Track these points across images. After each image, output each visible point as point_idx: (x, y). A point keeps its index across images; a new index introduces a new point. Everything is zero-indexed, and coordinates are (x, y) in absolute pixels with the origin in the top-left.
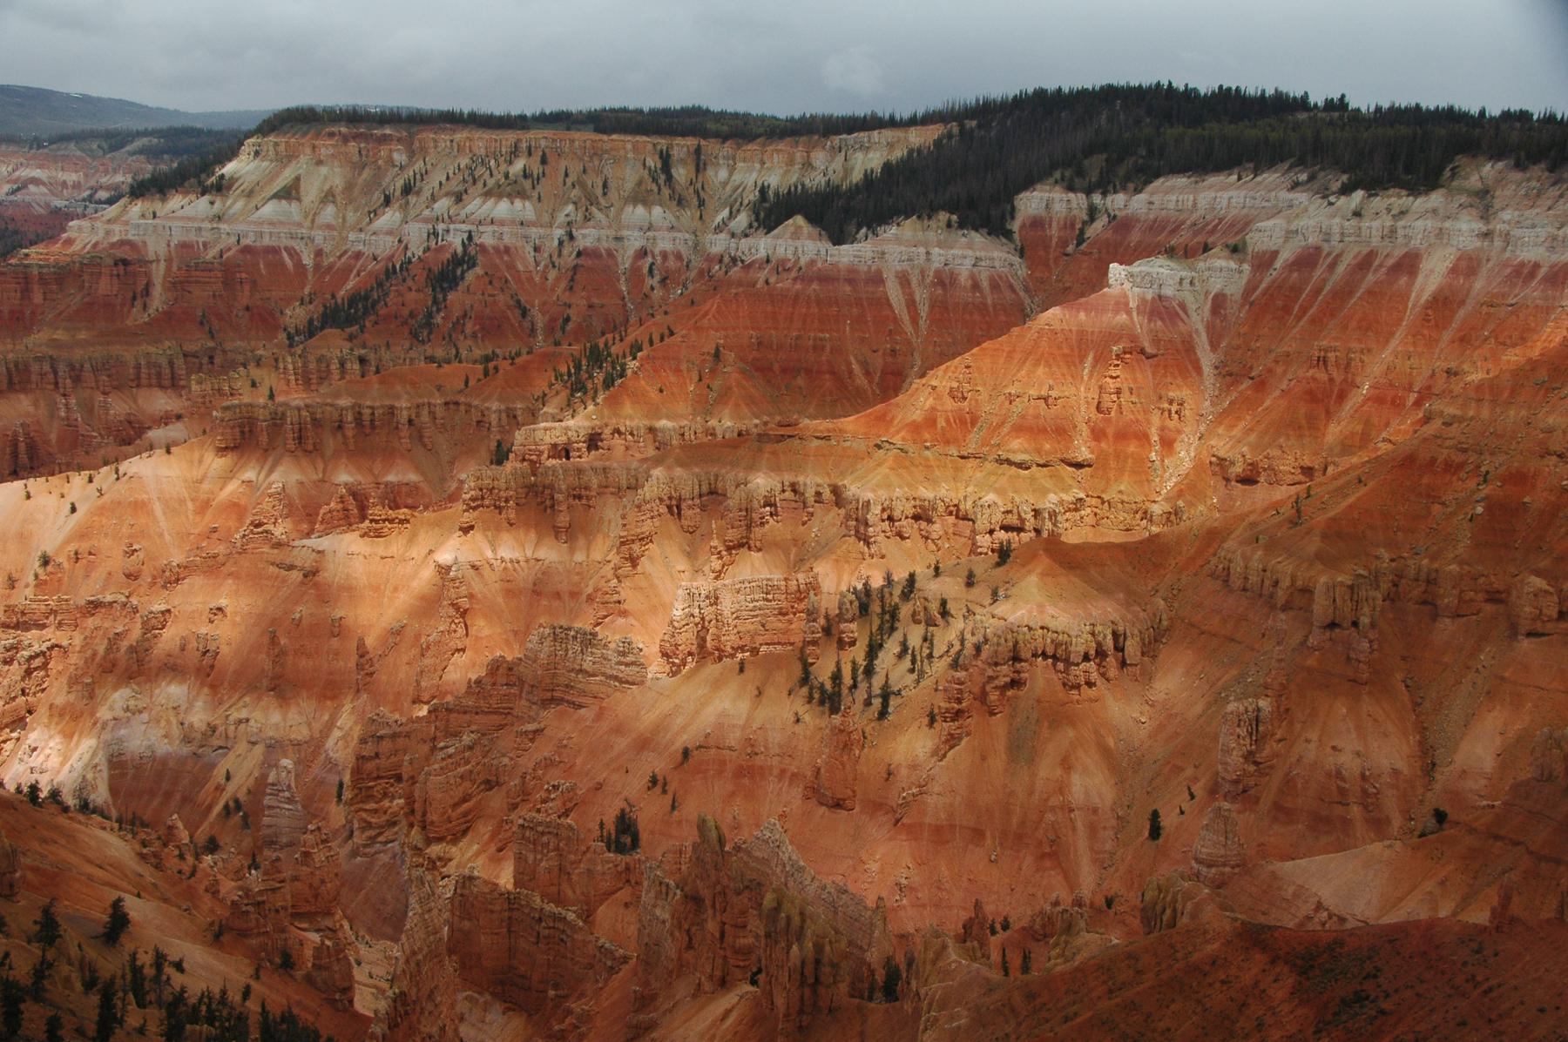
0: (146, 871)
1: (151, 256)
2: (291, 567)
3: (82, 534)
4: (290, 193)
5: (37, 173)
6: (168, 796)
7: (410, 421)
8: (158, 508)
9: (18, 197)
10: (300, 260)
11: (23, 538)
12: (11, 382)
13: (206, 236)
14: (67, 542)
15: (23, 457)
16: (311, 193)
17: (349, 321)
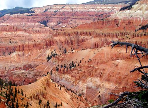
0: (71, 101)
1: (120, 19)
2: (115, 64)
3: (95, 57)
4: (140, 9)
5: (116, 8)
6: (93, 93)
7: (144, 44)
8: (105, 54)
9: (112, 11)
10: (141, 19)
11: (88, 57)
12: (97, 36)
13: (128, 16)
14: (93, 58)
15: (96, 46)
16: (144, 9)
17: (145, 29)
